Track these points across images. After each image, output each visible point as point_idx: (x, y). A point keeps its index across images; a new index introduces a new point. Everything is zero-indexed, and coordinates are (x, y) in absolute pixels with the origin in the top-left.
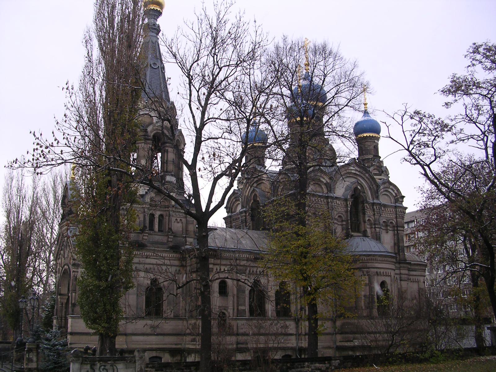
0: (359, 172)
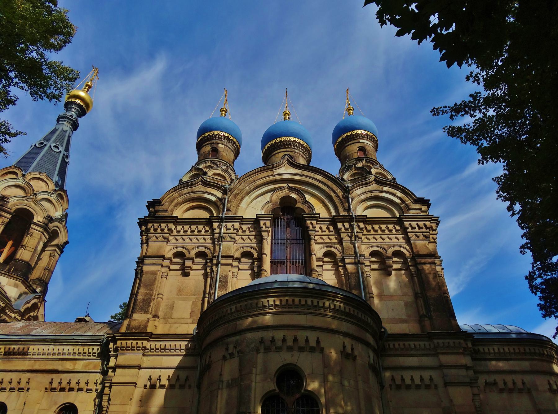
0: (300, 175)
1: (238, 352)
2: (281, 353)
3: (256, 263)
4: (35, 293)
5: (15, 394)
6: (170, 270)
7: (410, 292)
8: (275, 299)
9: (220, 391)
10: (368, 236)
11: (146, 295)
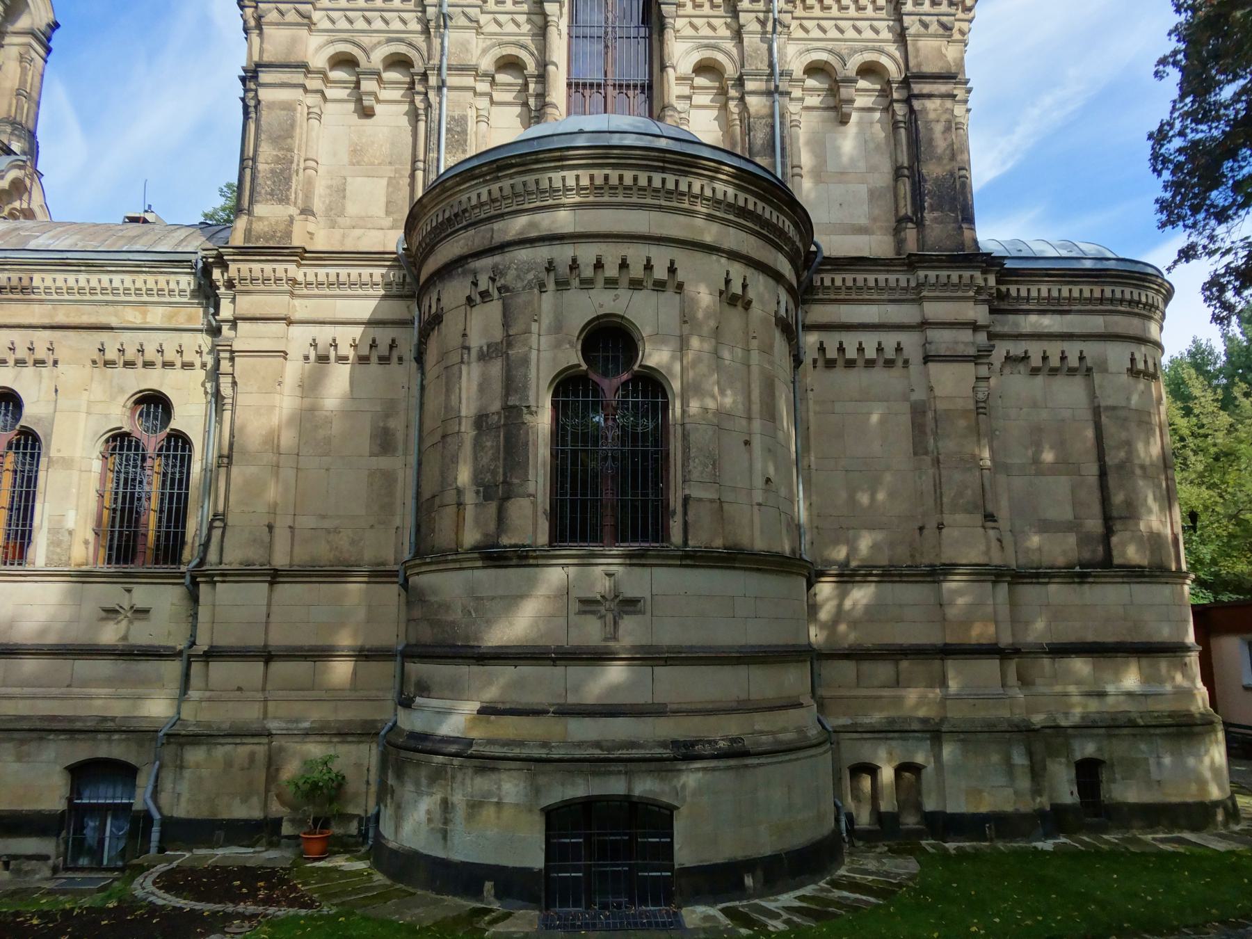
1: (499, 289)
2: (590, 291)
3: (532, 86)
4: (8, 154)
5: (29, 371)
6: (325, 99)
7: (886, 167)
8: (579, 172)
9: (464, 368)
10: (806, 23)
11: (278, 160)
